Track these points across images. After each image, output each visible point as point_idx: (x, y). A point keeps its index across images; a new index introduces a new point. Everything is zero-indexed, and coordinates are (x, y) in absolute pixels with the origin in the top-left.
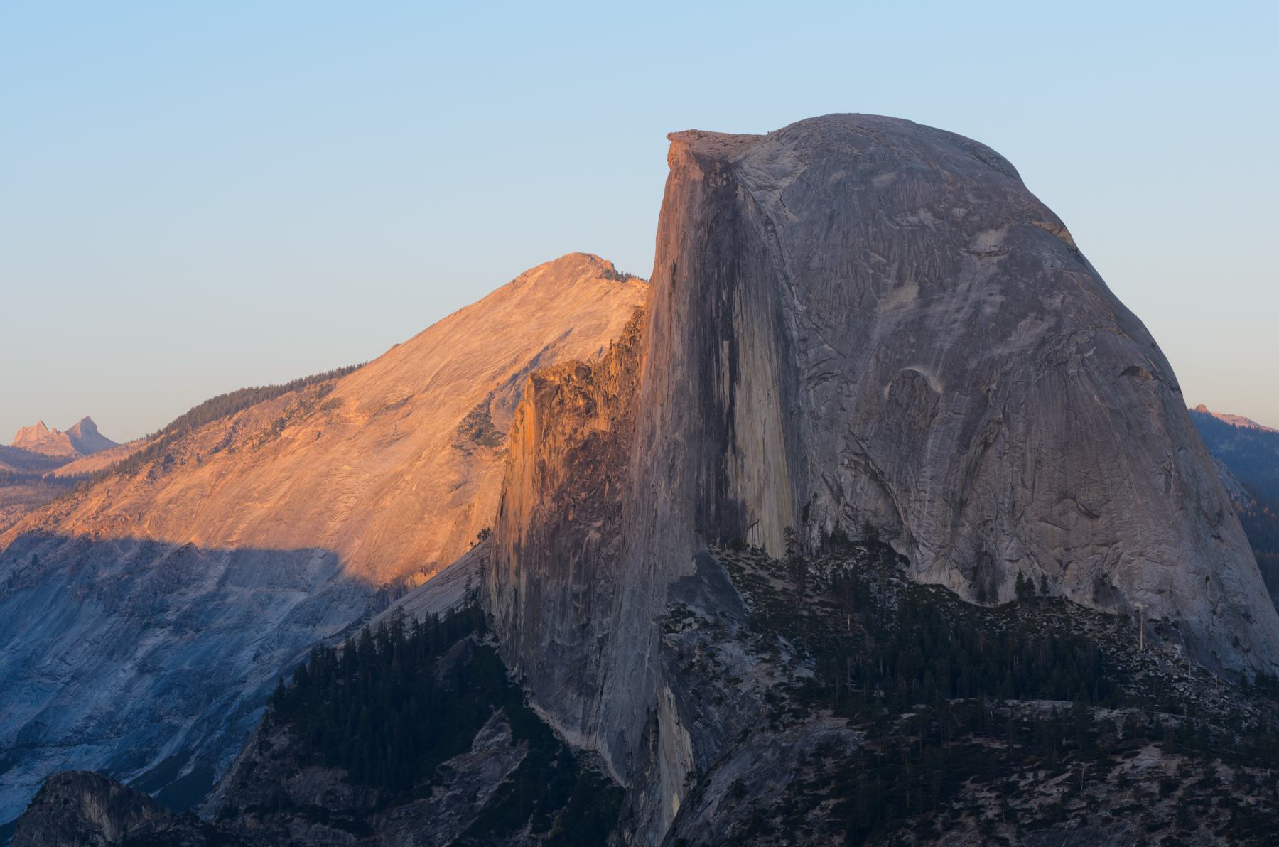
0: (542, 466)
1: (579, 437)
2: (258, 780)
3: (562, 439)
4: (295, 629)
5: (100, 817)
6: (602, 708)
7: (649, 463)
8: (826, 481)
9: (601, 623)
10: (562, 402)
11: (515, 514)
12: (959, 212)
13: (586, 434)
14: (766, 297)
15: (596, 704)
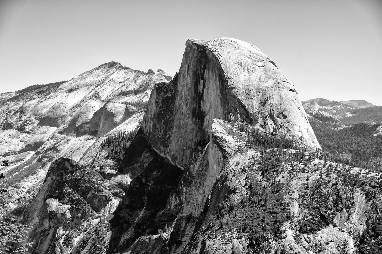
0: (157, 102)
1: (165, 97)
2: (99, 161)
3: (161, 97)
4: (57, 134)
5: (69, 166)
6: (168, 150)
7: (181, 103)
8: (233, 107)
9: (169, 133)
10: (161, 90)
11: (151, 111)
12: (254, 59)
13: (166, 96)
14: (216, 72)
15: (167, 149)
